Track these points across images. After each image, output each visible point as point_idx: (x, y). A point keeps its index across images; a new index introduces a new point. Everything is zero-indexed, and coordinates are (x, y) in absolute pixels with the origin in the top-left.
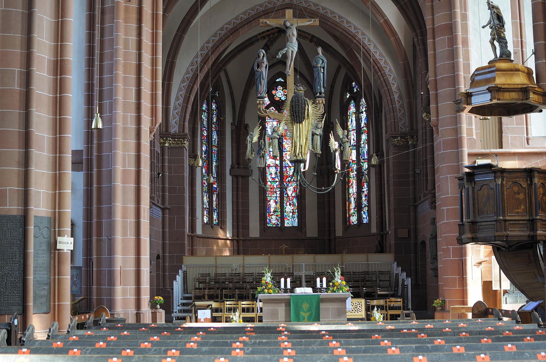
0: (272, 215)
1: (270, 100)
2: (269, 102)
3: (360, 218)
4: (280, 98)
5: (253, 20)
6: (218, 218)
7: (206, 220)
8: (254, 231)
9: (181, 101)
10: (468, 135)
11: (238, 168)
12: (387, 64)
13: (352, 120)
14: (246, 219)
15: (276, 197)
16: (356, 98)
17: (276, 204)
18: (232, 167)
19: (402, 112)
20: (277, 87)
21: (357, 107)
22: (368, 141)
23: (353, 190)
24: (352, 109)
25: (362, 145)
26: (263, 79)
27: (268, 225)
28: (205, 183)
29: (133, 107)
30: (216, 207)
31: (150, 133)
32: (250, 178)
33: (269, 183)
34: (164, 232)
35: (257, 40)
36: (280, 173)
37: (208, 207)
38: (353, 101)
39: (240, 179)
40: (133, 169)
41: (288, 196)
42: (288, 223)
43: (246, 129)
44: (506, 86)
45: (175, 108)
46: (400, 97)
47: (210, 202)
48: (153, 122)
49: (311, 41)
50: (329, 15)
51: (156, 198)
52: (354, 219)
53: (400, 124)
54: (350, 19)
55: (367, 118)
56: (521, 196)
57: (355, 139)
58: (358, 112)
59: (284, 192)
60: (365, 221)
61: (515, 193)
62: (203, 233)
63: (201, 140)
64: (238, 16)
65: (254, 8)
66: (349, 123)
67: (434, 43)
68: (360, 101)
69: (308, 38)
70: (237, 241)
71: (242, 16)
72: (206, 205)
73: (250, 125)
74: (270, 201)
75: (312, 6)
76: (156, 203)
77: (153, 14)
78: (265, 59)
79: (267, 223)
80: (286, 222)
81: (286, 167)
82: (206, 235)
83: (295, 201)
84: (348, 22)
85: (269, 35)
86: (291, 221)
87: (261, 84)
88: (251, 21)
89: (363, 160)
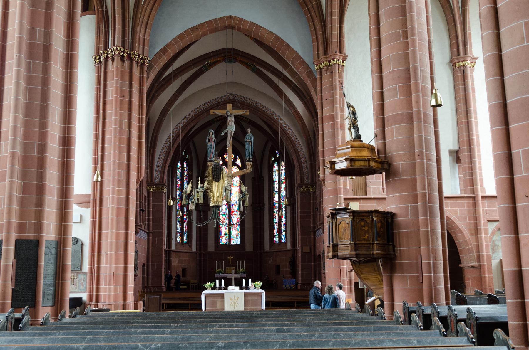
6: (187, 239)
7: (179, 240)
9: (161, 161)
10: (344, 186)
14: (206, 239)
21: (279, 166)
22: (286, 188)
23: (276, 220)
24: (276, 168)
25: (282, 191)
29: (125, 166)
31: (137, 183)
34: (148, 248)
40: (124, 207)
42: (233, 242)
44: (357, 158)
45: (157, 166)
46: (305, 160)
47: (182, 229)
48: (139, 176)
51: (143, 226)
52: (277, 240)
53: (305, 178)
54: (273, 110)
55: (286, 174)
56: (366, 228)
58: (279, 170)
60: (283, 241)
61: (362, 226)
62: (176, 248)
63: (176, 187)
65: (211, 101)
67: (323, 127)
70: (200, 254)
72: (179, 230)
76: (143, 229)
77: (140, 105)
78: (213, 136)
79: (219, 242)
80: (232, 241)
83: (238, 227)
84: (272, 111)
86: (236, 241)
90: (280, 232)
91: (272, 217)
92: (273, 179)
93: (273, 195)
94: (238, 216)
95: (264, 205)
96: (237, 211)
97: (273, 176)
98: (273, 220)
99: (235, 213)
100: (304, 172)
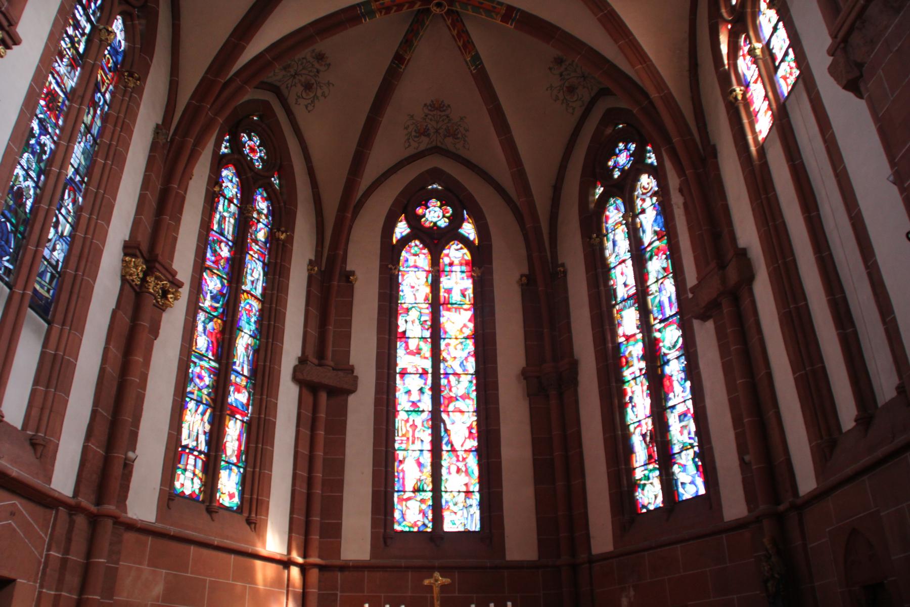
0: (409, 499)
1: (409, 226)
2: (408, 230)
3: (669, 484)
4: (435, 224)
7: (188, 482)
8: (356, 545)
11: (320, 365)
15: (421, 451)
17: (421, 471)
18: (302, 360)
25: (653, 288)
27: (397, 527)
28: (201, 378)
30: (238, 457)
32: (352, 399)
33: (401, 416)
36: (432, 389)
37: (203, 447)
39: (323, 397)
41: (453, 450)
43: (348, 280)
52: (650, 496)
57: (631, 281)
59: (441, 438)
66: (607, 253)
68: (634, 189)
73: (358, 274)
74: (401, 462)
80: (447, 516)
81: (446, 375)
82: (173, 530)
83: (472, 462)
89: (661, 321)
90: (664, 457)
91: (614, 400)
92: (604, 259)
93: (611, 318)
94: (471, 419)
95: (574, 365)
96: (465, 397)
97: (602, 249)
98: (623, 415)
99: (460, 404)
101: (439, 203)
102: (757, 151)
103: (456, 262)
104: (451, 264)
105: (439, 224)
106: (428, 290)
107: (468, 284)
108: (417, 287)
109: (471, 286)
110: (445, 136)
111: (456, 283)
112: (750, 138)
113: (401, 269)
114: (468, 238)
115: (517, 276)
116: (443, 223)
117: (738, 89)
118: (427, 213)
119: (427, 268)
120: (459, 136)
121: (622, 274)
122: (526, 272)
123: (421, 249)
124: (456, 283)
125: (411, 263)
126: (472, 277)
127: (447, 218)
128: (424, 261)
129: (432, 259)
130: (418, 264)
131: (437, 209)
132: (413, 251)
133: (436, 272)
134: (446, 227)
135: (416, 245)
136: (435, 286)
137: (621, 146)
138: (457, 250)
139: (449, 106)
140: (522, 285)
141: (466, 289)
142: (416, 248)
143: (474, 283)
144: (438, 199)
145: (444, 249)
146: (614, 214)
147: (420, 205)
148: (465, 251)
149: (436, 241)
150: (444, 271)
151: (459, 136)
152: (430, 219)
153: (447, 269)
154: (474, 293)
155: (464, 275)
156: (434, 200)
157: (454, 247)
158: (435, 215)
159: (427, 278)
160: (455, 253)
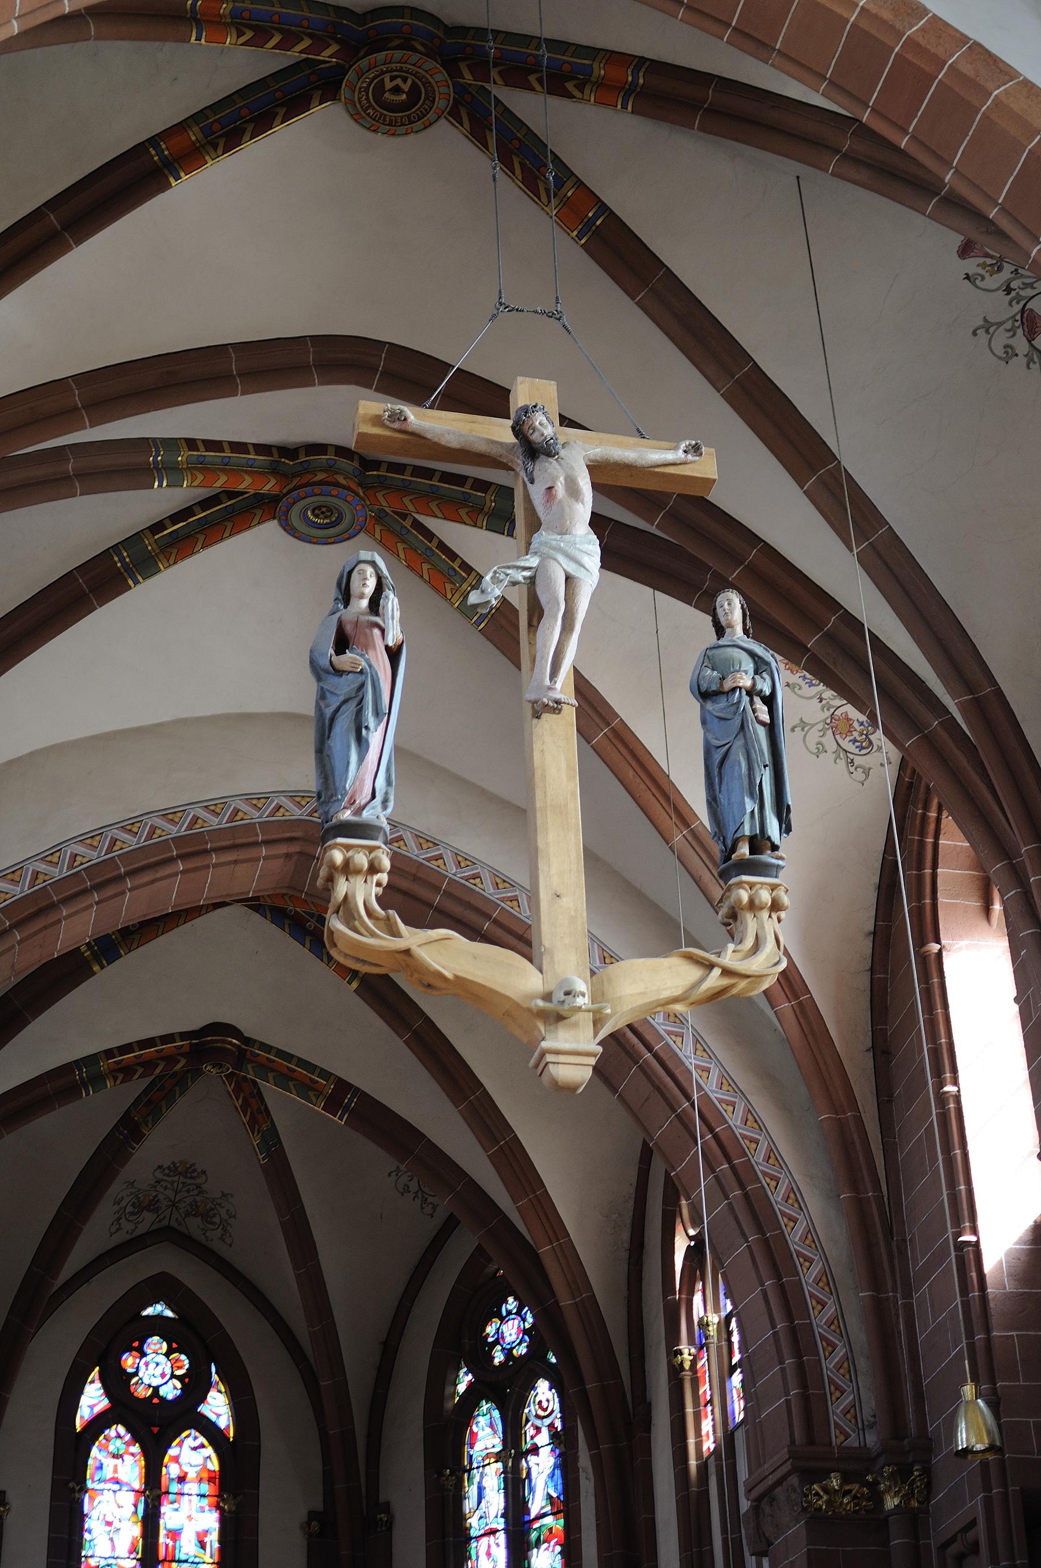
1: (108, 1392)
2: (105, 1403)
4: (156, 1389)
5: (131, 873)
12: (761, 1127)
13: (481, 1490)
16: (507, 1390)
19: (841, 1352)
20: (143, 1342)
26: (377, 713)
35: (97, 1080)
38: (485, 1406)
49: (333, 1104)
50: (488, 890)
53: (836, 1410)
58: (514, 1451)
64: (58, 848)
65: (137, 820)
66: (469, 1504)
68: (523, 1403)
69: (319, 1093)
71: (79, 849)
75: (412, 843)
85: (148, 1065)
87: (362, 743)
88: (119, 878)
92: (460, 1518)
97: (459, 1497)
100: (829, 1366)
101: (165, 1345)
102: (698, 1467)
103: (192, 1474)
104: (182, 1479)
105: (162, 1392)
106: (137, 1530)
107: (211, 1521)
108: (116, 1524)
109: (217, 1525)
110: (188, 1214)
111: (190, 1518)
112: (691, 1441)
113: (90, 1484)
114: (214, 1425)
115: (301, 1514)
116: (170, 1391)
117: (686, 1351)
118: (142, 1368)
119: (137, 1485)
120: (217, 1220)
121: (489, 1554)
122: (318, 1505)
123: (128, 1444)
124: (190, 1518)
125: (108, 1473)
126: (218, 1507)
127: (178, 1377)
128: (131, 1469)
129: (147, 1467)
130: (122, 1476)
131: (162, 1359)
132: (111, 1448)
133: (153, 1493)
134: (177, 1399)
135: (117, 1436)
136: (150, 1522)
137: (511, 1304)
138: (195, 1449)
139: (204, 1172)
140: (310, 1535)
141: (206, 1532)
142: (118, 1442)
143: (222, 1521)
144: (164, 1338)
145: (169, 1446)
146: (486, 1434)
147: (130, 1349)
148: (209, 1451)
149: (155, 1426)
150: (168, 1493)
151: (217, 1220)
152: (146, 1381)
153: (174, 1488)
154: (220, 1541)
155: (205, 1502)
156: (156, 1338)
157: (190, 1442)
158: (156, 1370)
159: (136, 1506)
160: (191, 1457)
